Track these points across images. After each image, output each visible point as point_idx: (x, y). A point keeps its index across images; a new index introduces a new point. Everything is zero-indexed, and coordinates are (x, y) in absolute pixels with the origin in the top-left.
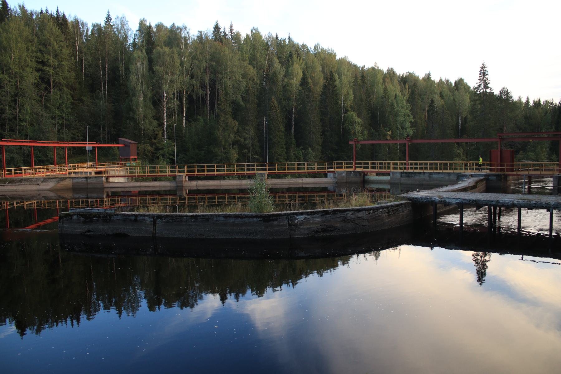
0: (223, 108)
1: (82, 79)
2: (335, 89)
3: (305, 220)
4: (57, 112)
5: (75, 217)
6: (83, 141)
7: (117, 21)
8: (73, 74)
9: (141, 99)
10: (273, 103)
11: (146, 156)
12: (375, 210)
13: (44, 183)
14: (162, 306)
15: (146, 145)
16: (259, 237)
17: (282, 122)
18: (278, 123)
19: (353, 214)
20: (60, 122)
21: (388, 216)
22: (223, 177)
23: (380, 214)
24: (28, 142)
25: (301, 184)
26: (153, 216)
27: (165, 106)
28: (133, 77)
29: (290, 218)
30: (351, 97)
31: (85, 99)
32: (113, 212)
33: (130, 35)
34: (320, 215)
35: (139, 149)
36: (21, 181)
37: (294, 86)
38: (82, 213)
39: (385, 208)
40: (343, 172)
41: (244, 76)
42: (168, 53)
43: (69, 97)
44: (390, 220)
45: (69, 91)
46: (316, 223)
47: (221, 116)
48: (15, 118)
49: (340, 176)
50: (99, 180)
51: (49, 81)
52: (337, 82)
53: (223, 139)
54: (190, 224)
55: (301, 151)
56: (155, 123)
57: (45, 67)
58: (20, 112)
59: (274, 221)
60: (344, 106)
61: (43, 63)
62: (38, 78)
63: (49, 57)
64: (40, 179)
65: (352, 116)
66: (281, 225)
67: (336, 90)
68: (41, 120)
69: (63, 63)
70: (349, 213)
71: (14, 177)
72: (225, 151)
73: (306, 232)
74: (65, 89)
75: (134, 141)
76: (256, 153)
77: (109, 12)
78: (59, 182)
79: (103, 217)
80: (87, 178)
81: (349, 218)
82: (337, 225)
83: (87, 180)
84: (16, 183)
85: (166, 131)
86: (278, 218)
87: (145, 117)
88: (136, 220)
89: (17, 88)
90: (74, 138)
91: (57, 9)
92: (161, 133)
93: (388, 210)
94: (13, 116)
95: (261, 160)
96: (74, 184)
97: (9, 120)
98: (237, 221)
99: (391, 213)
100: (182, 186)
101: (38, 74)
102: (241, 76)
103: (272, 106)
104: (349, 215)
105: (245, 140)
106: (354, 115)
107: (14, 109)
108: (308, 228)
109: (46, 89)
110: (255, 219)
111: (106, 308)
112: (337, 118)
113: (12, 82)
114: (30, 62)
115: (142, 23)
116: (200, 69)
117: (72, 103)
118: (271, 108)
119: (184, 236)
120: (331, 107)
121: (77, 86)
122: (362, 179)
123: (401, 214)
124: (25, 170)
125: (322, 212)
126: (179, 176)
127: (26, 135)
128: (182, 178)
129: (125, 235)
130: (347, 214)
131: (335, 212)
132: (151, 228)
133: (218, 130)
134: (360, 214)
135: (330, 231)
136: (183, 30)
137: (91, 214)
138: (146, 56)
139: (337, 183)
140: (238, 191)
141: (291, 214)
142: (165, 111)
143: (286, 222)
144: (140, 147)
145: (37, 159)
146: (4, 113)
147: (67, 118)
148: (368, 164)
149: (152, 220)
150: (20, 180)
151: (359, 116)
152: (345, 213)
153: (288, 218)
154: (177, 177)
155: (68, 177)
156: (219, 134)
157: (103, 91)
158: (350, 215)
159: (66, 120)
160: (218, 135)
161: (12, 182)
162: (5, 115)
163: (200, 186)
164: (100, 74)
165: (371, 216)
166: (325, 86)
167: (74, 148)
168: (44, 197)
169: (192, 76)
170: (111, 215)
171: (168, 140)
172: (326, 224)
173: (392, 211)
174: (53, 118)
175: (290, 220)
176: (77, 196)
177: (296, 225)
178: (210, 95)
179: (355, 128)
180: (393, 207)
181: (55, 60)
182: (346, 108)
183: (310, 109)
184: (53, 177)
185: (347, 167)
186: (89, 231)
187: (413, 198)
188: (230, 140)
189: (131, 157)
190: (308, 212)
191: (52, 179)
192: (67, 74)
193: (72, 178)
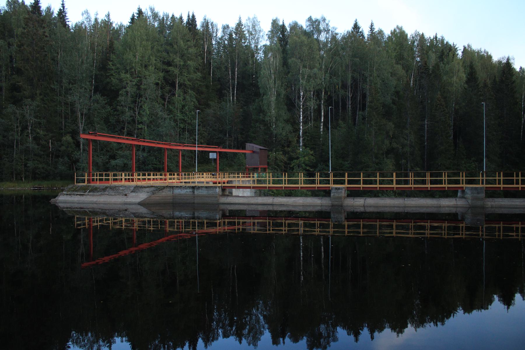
4: (179, 115)
7: (248, 23)
9: (273, 99)
11: (278, 167)
13: (134, 194)
14: (287, 340)
15: (277, 153)
20: (182, 126)
24: (123, 139)
27: (301, 107)
28: (265, 71)
33: (261, 36)
35: (270, 157)
36: (105, 189)
41: (393, 74)
42: (306, 42)
43: (194, 100)
45: (195, 94)
48: (134, 121)
51: (173, 85)
55: (473, 163)
56: (289, 127)
61: (169, 64)
62: (161, 78)
64: (128, 187)
71: (98, 184)
74: (190, 91)
75: (264, 147)
77: (240, 18)
80: (193, 188)
84: (98, 192)
85: (303, 137)
91: (189, 14)
92: (295, 139)
97: (128, 123)
101: (161, 74)
105: (403, 148)
107: (134, 111)
111: (226, 336)
113: (133, 81)
115: (275, 23)
116: (342, 66)
121: (204, 89)
126: (336, 188)
128: (341, 192)
136: (322, 22)
138: (280, 48)
144: (271, 155)
145: (152, 167)
147: (190, 121)
150: (104, 187)
154: (333, 191)
155: (167, 186)
157: (232, 97)
159: (188, 124)
161: (94, 190)
163: (370, 206)
168: (134, 214)
171: (304, 147)
178: (351, 97)
181: (181, 60)
191: (145, 187)
192: (194, 76)
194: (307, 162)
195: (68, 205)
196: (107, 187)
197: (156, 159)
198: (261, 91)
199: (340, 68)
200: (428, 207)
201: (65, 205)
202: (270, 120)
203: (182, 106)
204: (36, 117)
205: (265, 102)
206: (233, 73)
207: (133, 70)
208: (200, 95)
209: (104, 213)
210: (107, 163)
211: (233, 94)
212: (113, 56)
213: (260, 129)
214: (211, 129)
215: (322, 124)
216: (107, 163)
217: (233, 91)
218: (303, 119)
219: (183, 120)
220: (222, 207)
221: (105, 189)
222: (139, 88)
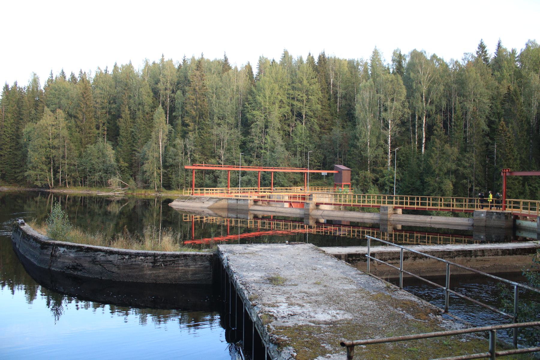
0: (439, 134)
10: (502, 126)
12: (132, 256)
19: (103, 256)
21: (153, 267)
23: (139, 263)
39: (150, 256)
46: (69, 259)
50: (245, 203)
70: (99, 254)
82: (85, 265)
93: (154, 259)
100: (309, 215)
103: (500, 130)
104: (99, 256)
122: (510, 223)
123: (180, 268)
133: (432, 158)
134: (111, 258)
140: (349, 224)
152: (96, 253)
156: (432, 162)
158: (100, 257)
160: (431, 163)
165: (124, 263)
167: (313, 173)
172: (76, 261)
173: (163, 261)
180: (166, 257)
202: (361, 145)
220: (252, 212)
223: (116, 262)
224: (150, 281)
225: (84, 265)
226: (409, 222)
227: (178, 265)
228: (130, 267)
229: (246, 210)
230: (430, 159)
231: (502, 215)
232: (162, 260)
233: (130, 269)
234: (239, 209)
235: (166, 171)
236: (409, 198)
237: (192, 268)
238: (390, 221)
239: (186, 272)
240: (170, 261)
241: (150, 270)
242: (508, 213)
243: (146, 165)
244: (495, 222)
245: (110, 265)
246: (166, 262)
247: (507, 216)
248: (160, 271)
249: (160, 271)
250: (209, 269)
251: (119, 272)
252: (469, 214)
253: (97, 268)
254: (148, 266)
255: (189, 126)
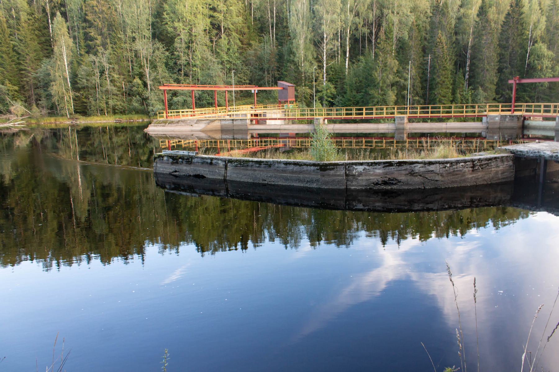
0: (382, 47)
1: (251, 23)
2: (522, 17)
3: (364, 171)
4: (226, 57)
5: (165, 158)
6: (250, 84)
8: (241, 19)
13: (196, 125)
16: (314, 185)
17: (450, 60)
18: (444, 61)
19: (422, 167)
20: (228, 66)
21: (472, 171)
22: (377, 121)
23: (460, 169)
25: (445, 129)
26: (224, 161)
29: (348, 167)
30: (543, 25)
31: (253, 44)
32: (194, 154)
34: (382, 166)
36: (178, 122)
37: (471, 17)
38: (170, 155)
39: (469, 162)
40: (497, 116)
43: (238, 41)
44: (474, 175)
45: (238, 36)
46: (376, 175)
47: (380, 55)
48: (188, 64)
49: (492, 121)
50: (243, 122)
51: (219, 28)
52: (526, 9)
53: (380, 80)
54: (255, 169)
57: (216, 13)
58: (193, 58)
59: (331, 170)
60: (531, 37)
61: (214, 9)
62: (209, 24)
63: (218, 3)
64: (194, 120)
65: (541, 48)
66: (338, 175)
67: (523, 18)
68: (210, 65)
69: (231, 8)
70: (417, 166)
71: (173, 119)
72: (382, 92)
73: (364, 184)
74: (234, 34)
76: (417, 94)
78: (209, 124)
79: (186, 159)
80: (233, 120)
81: (417, 172)
82: (401, 178)
83: (233, 123)
86: (335, 167)
87: (306, 59)
88: (211, 163)
89: (191, 35)
90: (241, 82)
93: (473, 164)
94: (187, 62)
95: (421, 102)
96: (222, 126)
98: (296, 168)
99: (477, 168)
101: (209, 21)
102: (409, 10)
103: (438, 42)
104: (417, 168)
106: (543, 48)
107: (188, 55)
108: (367, 180)
109: (217, 34)
110: (312, 168)
111: (272, 239)
112: (520, 51)
114: (201, 9)
116: (364, 6)
117: (240, 48)
118: (437, 44)
119: (249, 181)
120: (513, 39)
121: (246, 30)
124: (183, 112)
125: (384, 163)
126: (317, 119)
127: (198, 80)
129: (203, 177)
130: (414, 167)
131: (400, 164)
132: (223, 171)
133: (376, 71)
134: (432, 168)
135: (393, 184)
137: (177, 156)
139: (487, 128)
141: (350, 164)
142: (325, 53)
143: (344, 172)
146: (179, 60)
147: (234, 62)
148: (549, 106)
149: (224, 163)
151: (549, 48)
152: (413, 166)
153: (346, 168)
154: (315, 120)
156: (377, 75)
160: (375, 76)
161: (171, 123)
162: (180, 61)
163: (337, 130)
164: (269, 17)
165: (447, 170)
166: (508, 14)
167: (241, 91)
168: (197, 137)
169: (357, 15)
170: (192, 158)
171: (327, 82)
174: (222, 63)
175: (348, 170)
176: (225, 137)
177: (354, 176)
179: (542, 63)
180: (482, 161)
182: (534, 39)
183: (485, 43)
184: (206, 119)
185: (502, 111)
186: (176, 171)
187: (517, 151)
188: (388, 81)
189: (289, 100)
190: (368, 163)
193: (220, 120)
194: (329, 95)
195: (156, 133)
196: (179, 121)
197: (209, 96)
198: (291, 35)
199: (363, 8)
200: (371, 129)
201: (154, 133)
202: (298, 61)
203: (228, 49)
204: (110, 63)
205: (294, 45)
206: (272, 12)
207: (185, 19)
208: (243, 36)
209: (179, 138)
210: (171, 100)
211: (273, 32)
212: (166, 6)
213: (291, 67)
214: (252, 68)
215: (347, 59)
216: (171, 100)
217: (273, 29)
218: (326, 58)
219: (228, 61)
220: (251, 132)
221: (178, 122)
222: (191, 35)
223: (438, 171)
224: (472, 184)
225: (399, 178)
226: (425, 129)
227: (491, 167)
228: (453, 173)
229: (245, 130)
230: (374, 72)
231: (514, 117)
232: (479, 164)
233: (453, 175)
234: (236, 130)
235: (79, 94)
236: (453, 107)
237: (501, 168)
238: (406, 129)
239: (497, 172)
240: (485, 164)
241: (471, 174)
242: (520, 115)
243: (55, 88)
244: (508, 123)
245: (432, 175)
246: (482, 165)
247: (518, 117)
248: (479, 174)
249: (479, 174)
250: (512, 167)
251: (443, 179)
252: (479, 119)
253: (417, 179)
254: (469, 171)
255: (97, 39)
